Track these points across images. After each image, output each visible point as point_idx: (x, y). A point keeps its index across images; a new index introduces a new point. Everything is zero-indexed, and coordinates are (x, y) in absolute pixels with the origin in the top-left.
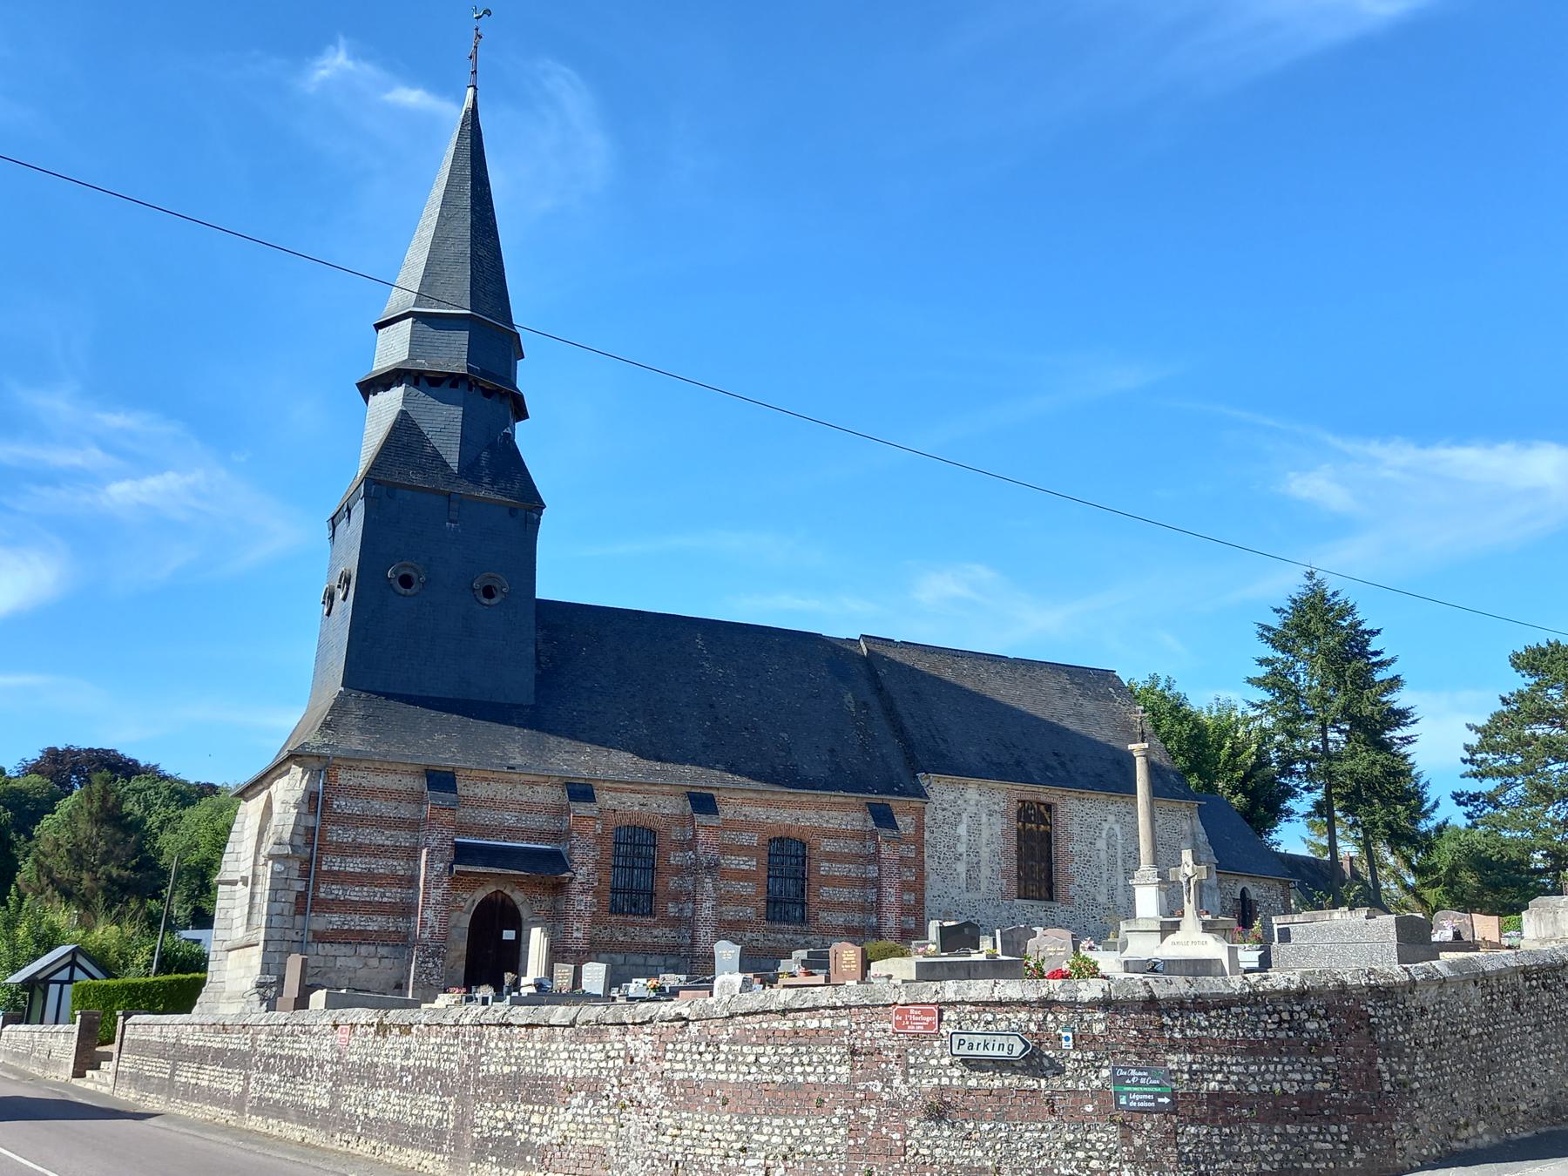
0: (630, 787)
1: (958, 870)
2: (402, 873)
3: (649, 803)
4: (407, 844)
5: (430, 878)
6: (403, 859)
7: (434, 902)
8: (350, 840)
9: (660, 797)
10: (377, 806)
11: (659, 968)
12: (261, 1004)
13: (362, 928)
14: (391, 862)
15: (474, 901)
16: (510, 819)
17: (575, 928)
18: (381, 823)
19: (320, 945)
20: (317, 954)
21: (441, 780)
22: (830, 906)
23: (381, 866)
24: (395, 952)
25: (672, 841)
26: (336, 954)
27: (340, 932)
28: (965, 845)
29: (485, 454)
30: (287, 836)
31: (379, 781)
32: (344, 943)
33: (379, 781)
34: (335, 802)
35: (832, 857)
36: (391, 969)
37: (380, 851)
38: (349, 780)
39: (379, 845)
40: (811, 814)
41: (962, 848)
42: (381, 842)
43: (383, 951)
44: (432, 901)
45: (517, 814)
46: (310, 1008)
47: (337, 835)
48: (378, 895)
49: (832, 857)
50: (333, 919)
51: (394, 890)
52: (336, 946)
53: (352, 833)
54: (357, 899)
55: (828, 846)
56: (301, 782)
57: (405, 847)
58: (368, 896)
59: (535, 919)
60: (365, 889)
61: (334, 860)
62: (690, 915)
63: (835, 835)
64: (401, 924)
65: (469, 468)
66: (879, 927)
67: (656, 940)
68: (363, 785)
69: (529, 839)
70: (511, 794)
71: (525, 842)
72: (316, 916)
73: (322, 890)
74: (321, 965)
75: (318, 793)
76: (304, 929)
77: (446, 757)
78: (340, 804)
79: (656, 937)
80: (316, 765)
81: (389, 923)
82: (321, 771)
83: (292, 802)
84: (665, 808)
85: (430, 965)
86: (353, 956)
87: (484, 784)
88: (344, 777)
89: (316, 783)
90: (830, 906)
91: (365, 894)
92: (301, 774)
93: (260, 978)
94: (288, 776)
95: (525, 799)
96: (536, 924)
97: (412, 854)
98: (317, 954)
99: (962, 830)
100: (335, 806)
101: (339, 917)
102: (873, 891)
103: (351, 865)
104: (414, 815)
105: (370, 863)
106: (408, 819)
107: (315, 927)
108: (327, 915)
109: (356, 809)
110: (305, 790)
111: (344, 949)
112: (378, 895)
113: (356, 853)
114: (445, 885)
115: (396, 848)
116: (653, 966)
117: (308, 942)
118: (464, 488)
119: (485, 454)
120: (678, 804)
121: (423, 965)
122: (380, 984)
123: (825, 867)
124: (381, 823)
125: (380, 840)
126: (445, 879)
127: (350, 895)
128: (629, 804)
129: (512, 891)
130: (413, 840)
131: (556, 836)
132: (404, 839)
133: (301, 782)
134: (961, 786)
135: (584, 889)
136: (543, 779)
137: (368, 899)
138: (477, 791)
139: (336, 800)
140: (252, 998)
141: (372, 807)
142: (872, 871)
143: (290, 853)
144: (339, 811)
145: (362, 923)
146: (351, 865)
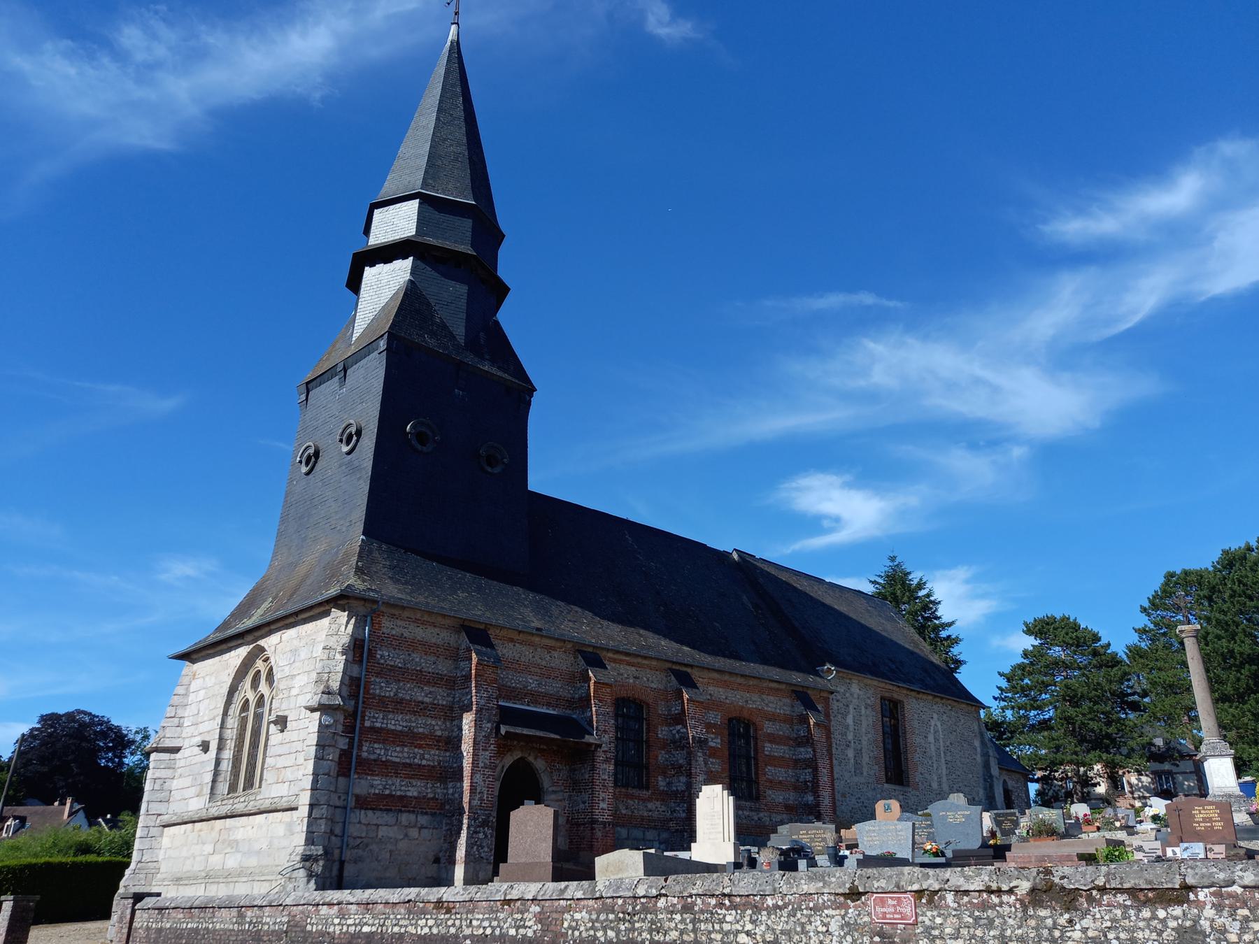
0: (627, 659)
1: (849, 755)
2: (439, 733)
3: (641, 676)
4: (444, 703)
5: (478, 739)
6: (440, 718)
7: (483, 765)
8: (392, 694)
9: (648, 671)
10: (418, 660)
11: (654, 842)
12: (308, 882)
13: (402, 793)
14: (429, 721)
15: (503, 767)
16: (532, 683)
17: (601, 798)
18: (421, 678)
19: (363, 812)
20: (360, 822)
21: (479, 636)
22: (773, 784)
23: (421, 725)
24: (434, 821)
25: (660, 715)
26: (378, 823)
27: (380, 797)
28: (852, 733)
29: (482, 334)
30: (335, 685)
31: (419, 633)
32: (386, 810)
33: (419, 633)
34: (379, 652)
35: (773, 739)
36: (430, 840)
37: (420, 709)
38: (392, 628)
39: (419, 702)
40: (755, 697)
41: (850, 737)
42: (420, 699)
43: (423, 820)
44: (481, 765)
45: (537, 678)
46: (455, 885)
47: (384, 688)
48: (418, 757)
49: (773, 739)
50: (375, 782)
51: (433, 752)
52: (378, 813)
53: (394, 686)
54: (398, 760)
55: (769, 727)
56: (346, 626)
57: (443, 705)
58: (409, 758)
59: (554, 788)
60: (406, 749)
61: (377, 715)
62: (684, 788)
63: (773, 718)
64: (439, 791)
65: (472, 344)
66: (818, 805)
67: (650, 813)
68: (405, 635)
69: (548, 705)
70: (533, 657)
71: (545, 707)
72: (359, 778)
73: (365, 748)
74: (363, 835)
75: (364, 641)
76: (348, 794)
77: (478, 612)
78: (385, 655)
79: (650, 811)
80: (362, 610)
81: (427, 788)
82: (366, 616)
83: (339, 649)
84: (652, 682)
85: (481, 836)
86: (395, 825)
87: (511, 645)
88: (389, 626)
89: (361, 630)
90: (773, 784)
91: (405, 755)
92: (347, 619)
93: (305, 850)
94: (329, 618)
95: (544, 663)
96: (711, 780)
97: (453, 715)
98: (360, 822)
99: (850, 720)
100: (379, 656)
101: (381, 781)
102: (806, 771)
103: (393, 722)
104: (451, 672)
105: (410, 721)
106: (445, 675)
107: (357, 791)
108: (369, 778)
109: (398, 660)
110: (352, 636)
111: (389, 818)
112: (418, 757)
113: (398, 709)
114: (492, 746)
115: (435, 706)
116: (650, 840)
117: (351, 808)
118: (469, 359)
119: (482, 334)
120: (662, 679)
121: (474, 836)
122: (420, 858)
123: (768, 748)
124: (421, 678)
125: (420, 696)
126: (492, 741)
127: (391, 756)
128: (626, 676)
129: (535, 759)
130: (450, 699)
131: (570, 703)
132: (441, 696)
133: (346, 626)
134: (848, 681)
135: (607, 758)
136: (559, 644)
137: (408, 761)
138: (505, 651)
139: (380, 650)
140: (295, 874)
141: (412, 660)
142: (805, 753)
143: (342, 704)
144: (382, 661)
145: (403, 788)
146: (393, 722)
